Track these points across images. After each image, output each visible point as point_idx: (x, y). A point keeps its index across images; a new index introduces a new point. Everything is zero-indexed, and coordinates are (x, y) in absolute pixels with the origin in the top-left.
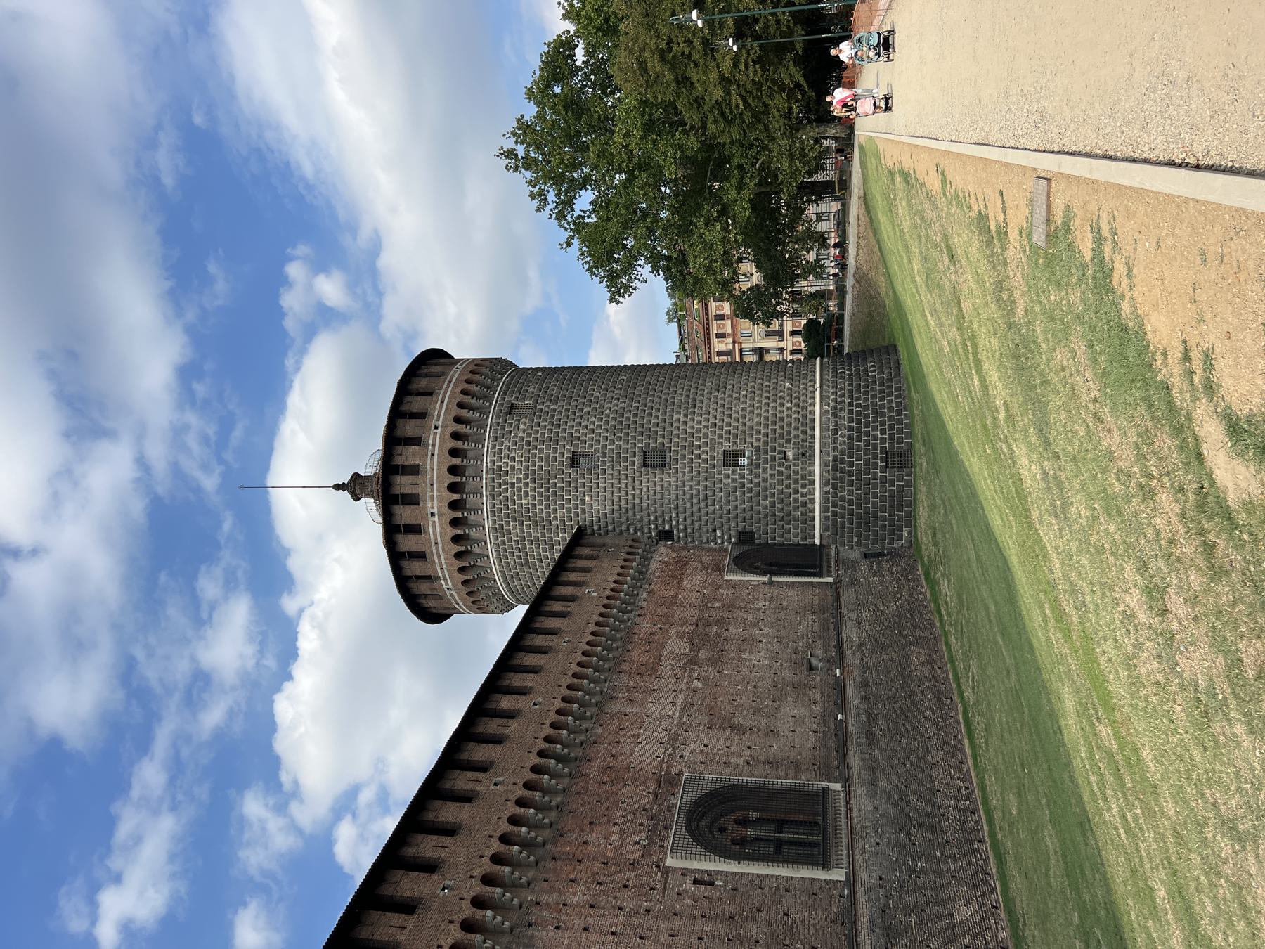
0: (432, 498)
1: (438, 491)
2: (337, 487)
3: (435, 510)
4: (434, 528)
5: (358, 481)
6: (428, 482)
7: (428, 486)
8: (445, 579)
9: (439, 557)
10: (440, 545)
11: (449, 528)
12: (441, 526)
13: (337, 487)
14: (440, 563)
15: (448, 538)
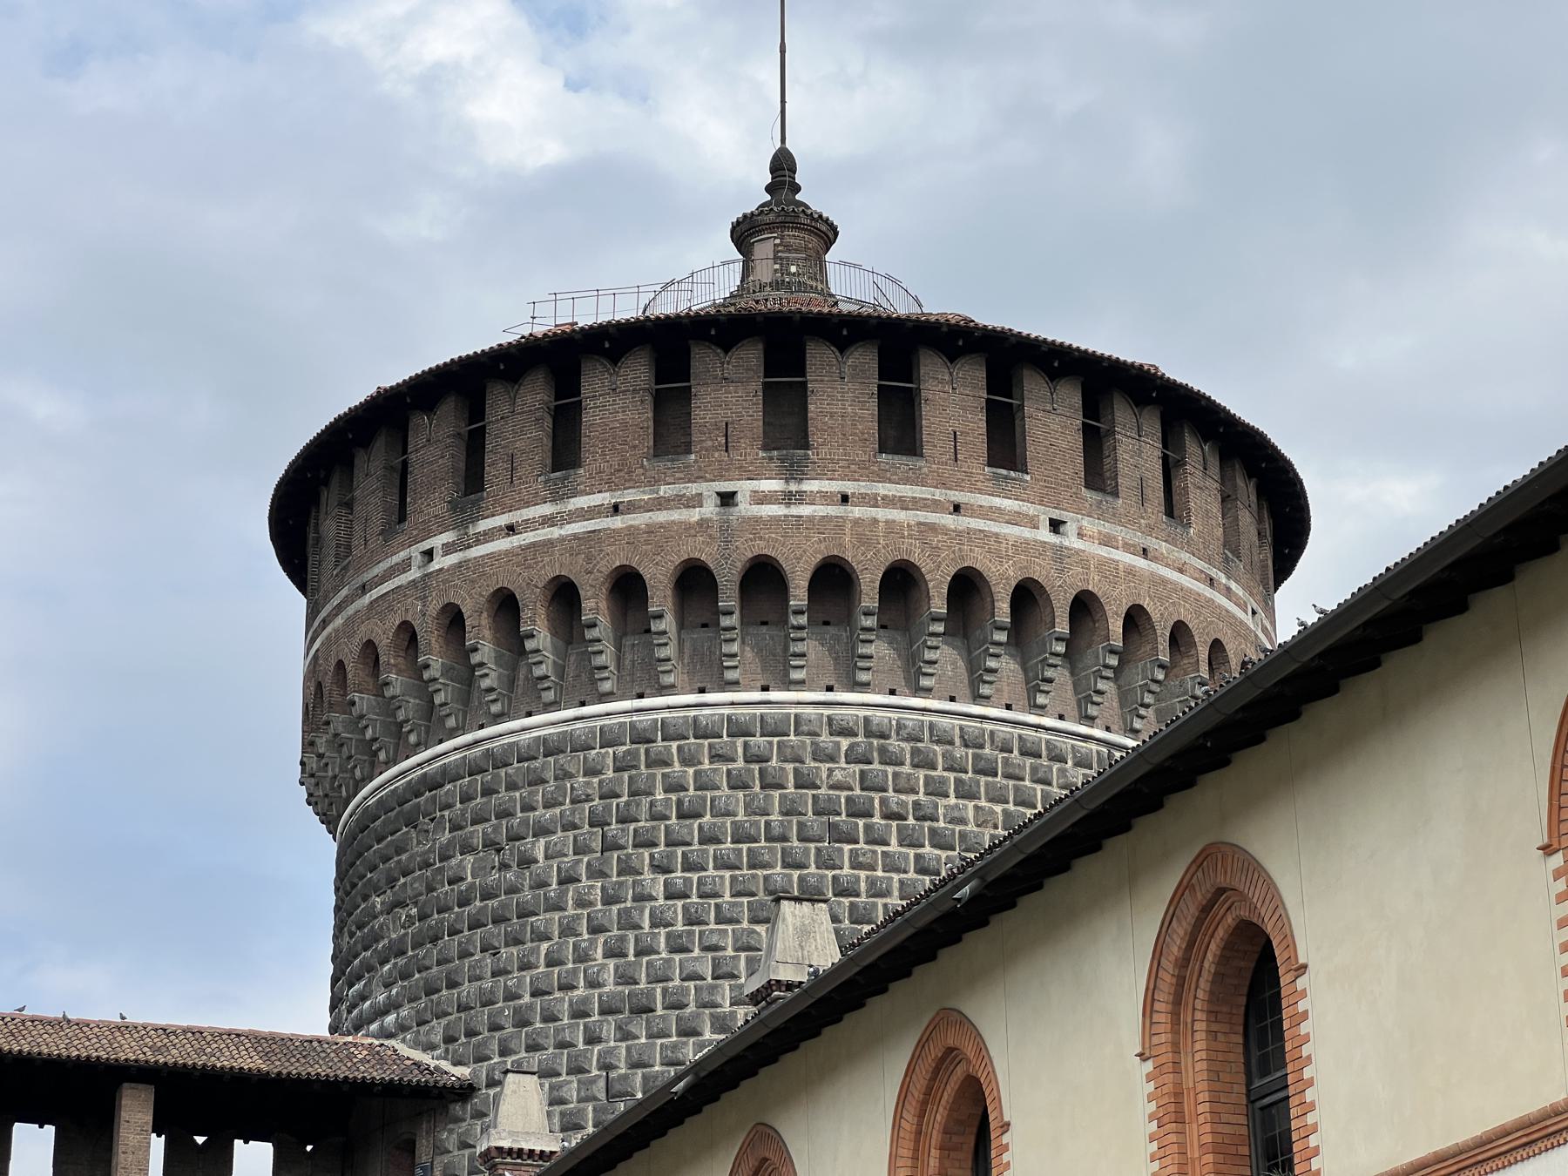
0: (1107, 541)
1: (1131, 571)
2: (783, 165)
3: (1071, 541)
4: (1015, 519)
5: (814, 242)
6: (1152, 543)
7: (1139, 539)
8: (789, 498)
9: (889, 502)
10: (949, 520)
11: (1014, 576)
12: (1023, 546)
13: (783, 165)
14: (873, 501)
15: (1041, 571)
